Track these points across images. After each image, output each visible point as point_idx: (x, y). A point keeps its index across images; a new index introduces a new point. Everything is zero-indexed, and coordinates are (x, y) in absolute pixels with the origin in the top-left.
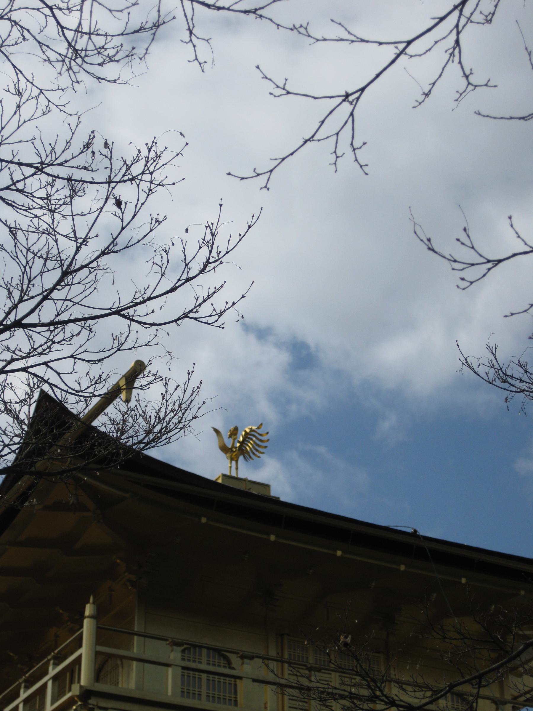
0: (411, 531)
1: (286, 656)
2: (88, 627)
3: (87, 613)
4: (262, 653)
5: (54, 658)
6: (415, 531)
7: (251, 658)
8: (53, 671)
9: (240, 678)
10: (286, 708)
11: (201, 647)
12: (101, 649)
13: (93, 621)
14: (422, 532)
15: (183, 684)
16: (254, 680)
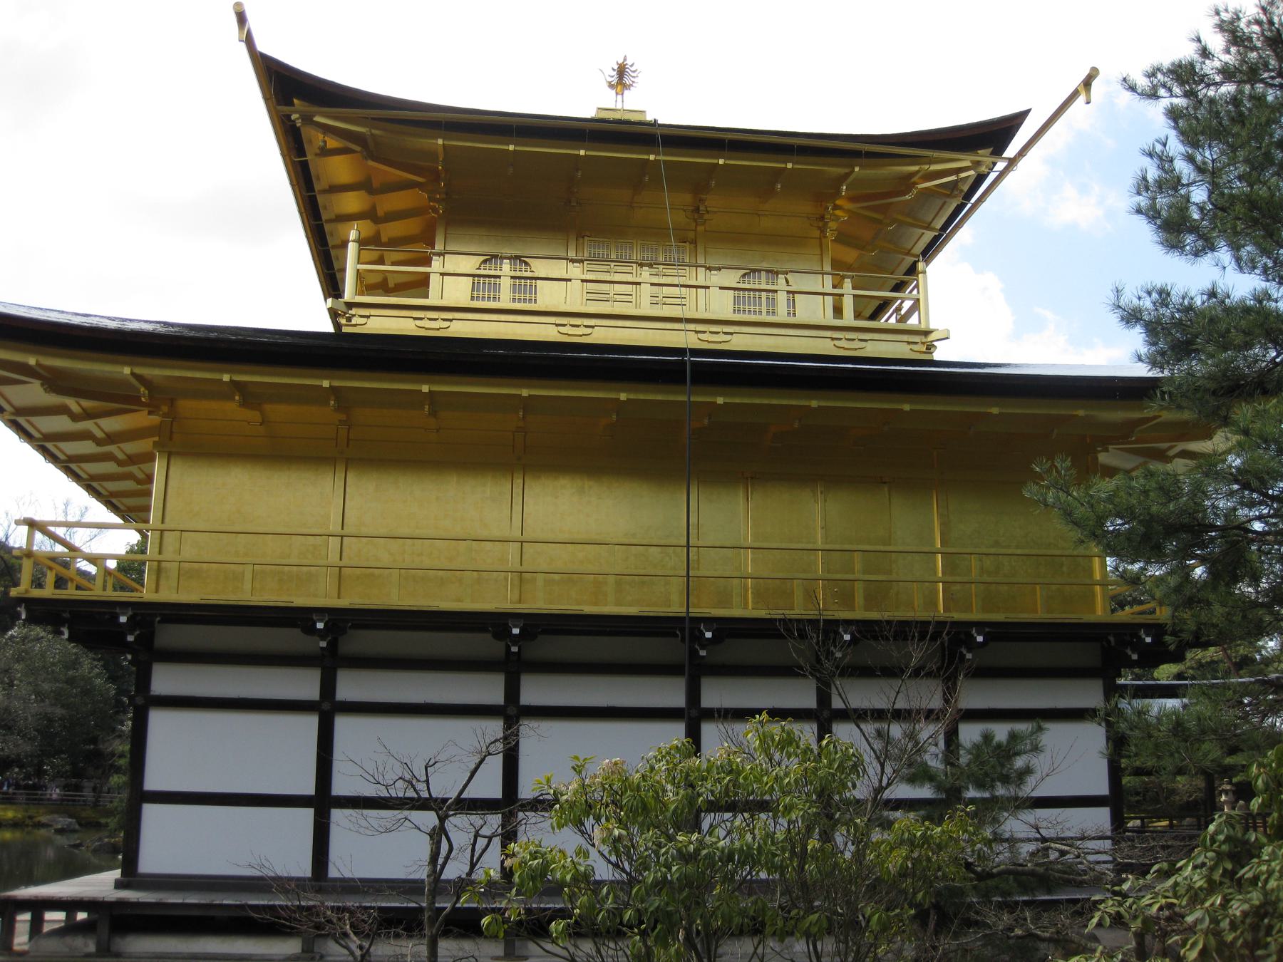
4: (563, 254)
11: (759, 271)
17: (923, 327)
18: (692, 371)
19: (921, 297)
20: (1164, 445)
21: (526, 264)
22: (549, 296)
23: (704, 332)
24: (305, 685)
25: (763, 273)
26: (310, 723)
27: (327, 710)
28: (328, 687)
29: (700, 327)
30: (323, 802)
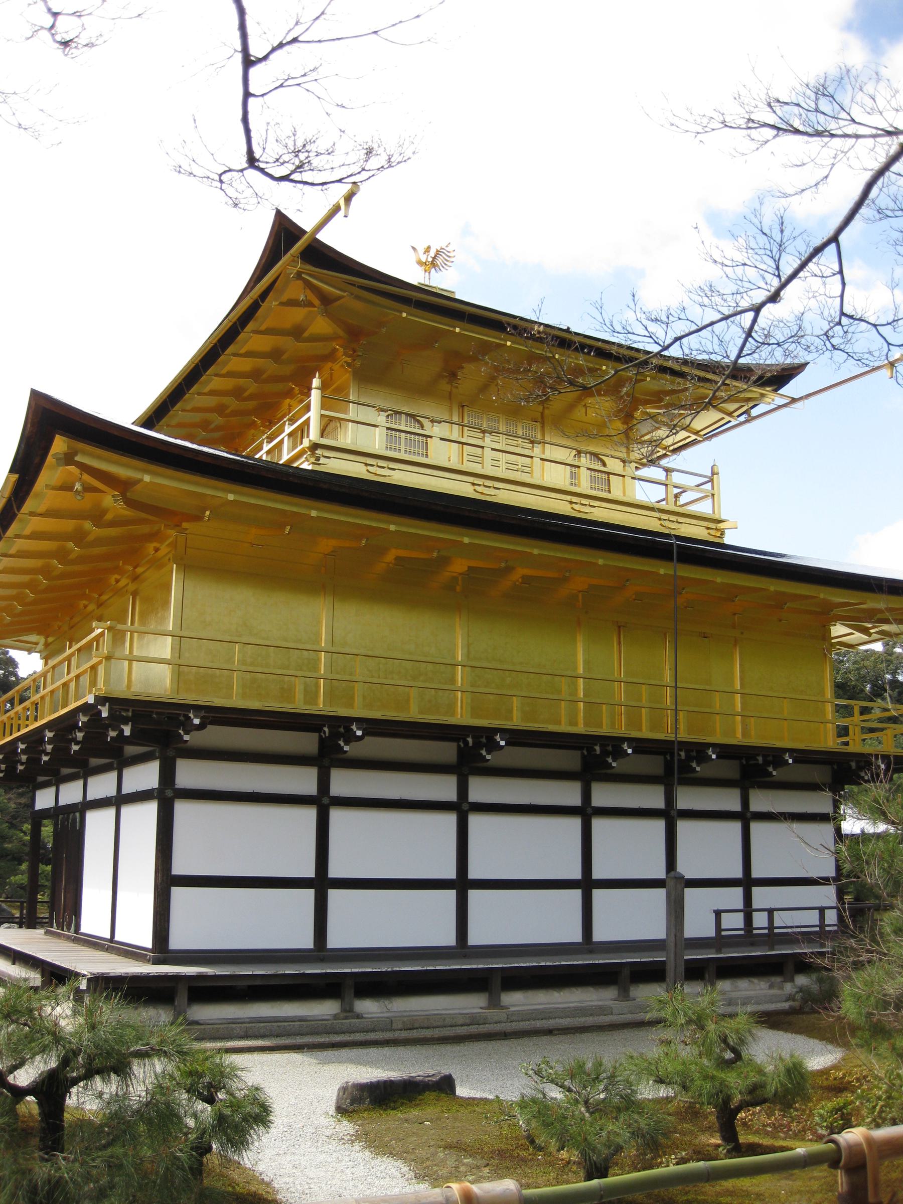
0: (565, 328)
1: (466, 421)
2: (315, 396)
3: (314, 385)
4: (447, 418)
5: (289, 420)
6: (569, 328)
7: (440, 422)
8: (288, 429)
9: (431, 437)
10: (465, 461)
11: (400, 413)
12: (324, 412)
13: (319, 392)
14: (573, 329)
15: (387, 442)
16: (442, 439)
17: (716, 517)
18: (678, 552)
19: (715, 492)
20: (870, 625)
21: (419, 422)
22: (442, 453)
23: (576, 503)
24: (303, 780)
25: (588, 455)
26: (309, 815)
27: (323, 803)
28: (324, 783)
29: (575, 499)
30: (321, 883)
